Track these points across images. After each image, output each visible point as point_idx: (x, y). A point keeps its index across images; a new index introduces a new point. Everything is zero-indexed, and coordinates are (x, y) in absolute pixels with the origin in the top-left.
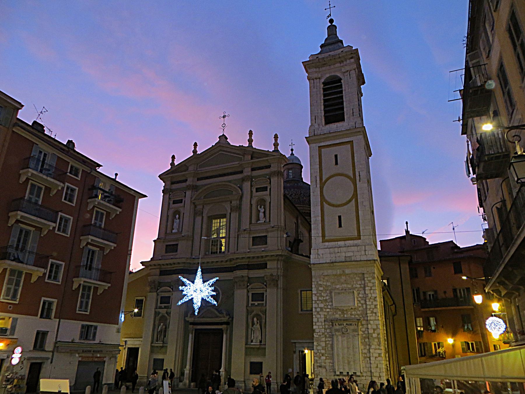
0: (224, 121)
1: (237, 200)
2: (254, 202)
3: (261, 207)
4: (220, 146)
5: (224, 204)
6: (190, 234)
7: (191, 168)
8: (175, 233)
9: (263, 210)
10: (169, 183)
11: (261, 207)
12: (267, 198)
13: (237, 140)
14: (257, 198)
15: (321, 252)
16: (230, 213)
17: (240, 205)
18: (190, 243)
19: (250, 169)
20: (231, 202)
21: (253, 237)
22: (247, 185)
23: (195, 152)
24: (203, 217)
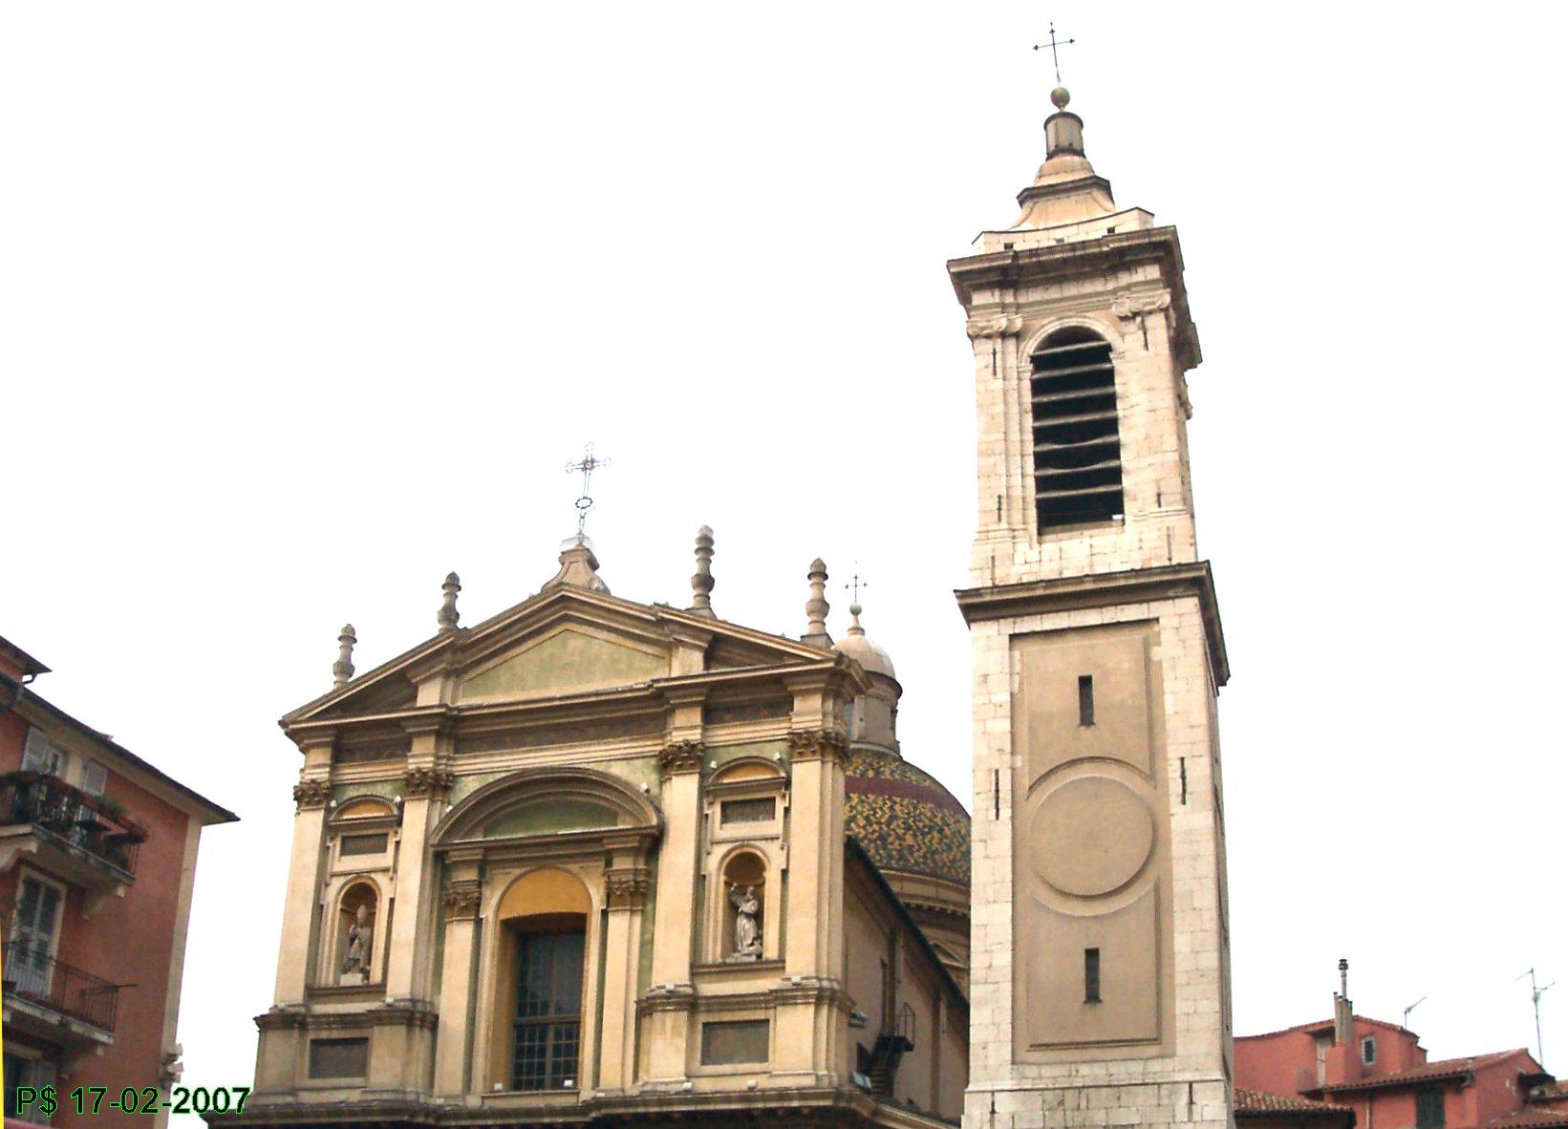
0: (586, 484)
1: (635, 852)
2: (713, 863)
5: (574, 867)
10: (322, 756)
12: (774, 859)
13: (646, 574)
15: (1005, 1105)
16: (605, 914)
17: (652, 874)
19: (696, 717)
20: (609, 863)
21: (705, 1025)
23: (449, 614)
24: (479, 923)
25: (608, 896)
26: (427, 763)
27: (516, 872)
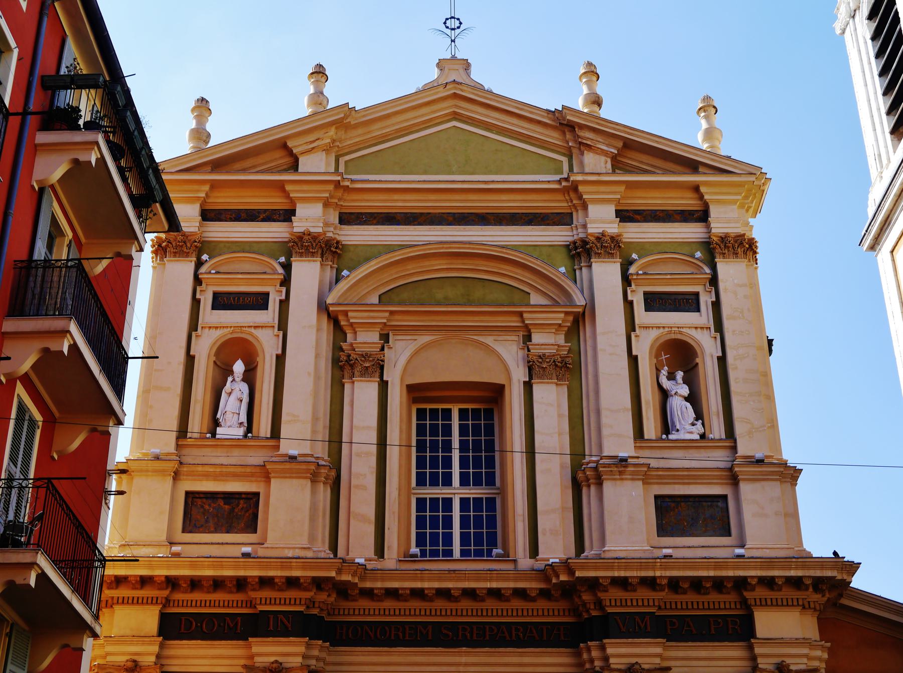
2: (643, 347)
3: (671, 377)
4: (455, 96)
5: (489, 340)
6: (321, 451)
7: (315, 164)
8: (232, 444)
9: (685, 390)
11: (671, 377)
14: (654, 334)
18: (324, 494)
19: (610, 211)
20: (528, 338)
22: (605, 274)
25: (530, 369)
26: (317, 229)
27: (425, 339)
